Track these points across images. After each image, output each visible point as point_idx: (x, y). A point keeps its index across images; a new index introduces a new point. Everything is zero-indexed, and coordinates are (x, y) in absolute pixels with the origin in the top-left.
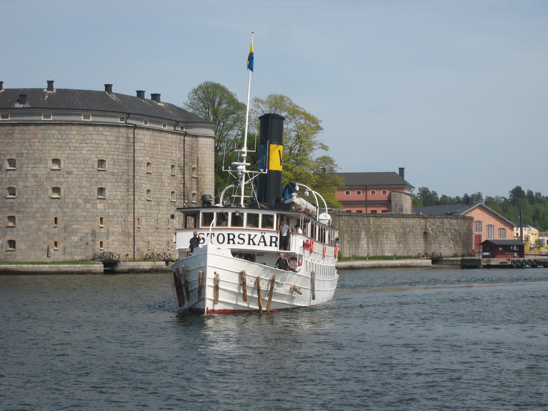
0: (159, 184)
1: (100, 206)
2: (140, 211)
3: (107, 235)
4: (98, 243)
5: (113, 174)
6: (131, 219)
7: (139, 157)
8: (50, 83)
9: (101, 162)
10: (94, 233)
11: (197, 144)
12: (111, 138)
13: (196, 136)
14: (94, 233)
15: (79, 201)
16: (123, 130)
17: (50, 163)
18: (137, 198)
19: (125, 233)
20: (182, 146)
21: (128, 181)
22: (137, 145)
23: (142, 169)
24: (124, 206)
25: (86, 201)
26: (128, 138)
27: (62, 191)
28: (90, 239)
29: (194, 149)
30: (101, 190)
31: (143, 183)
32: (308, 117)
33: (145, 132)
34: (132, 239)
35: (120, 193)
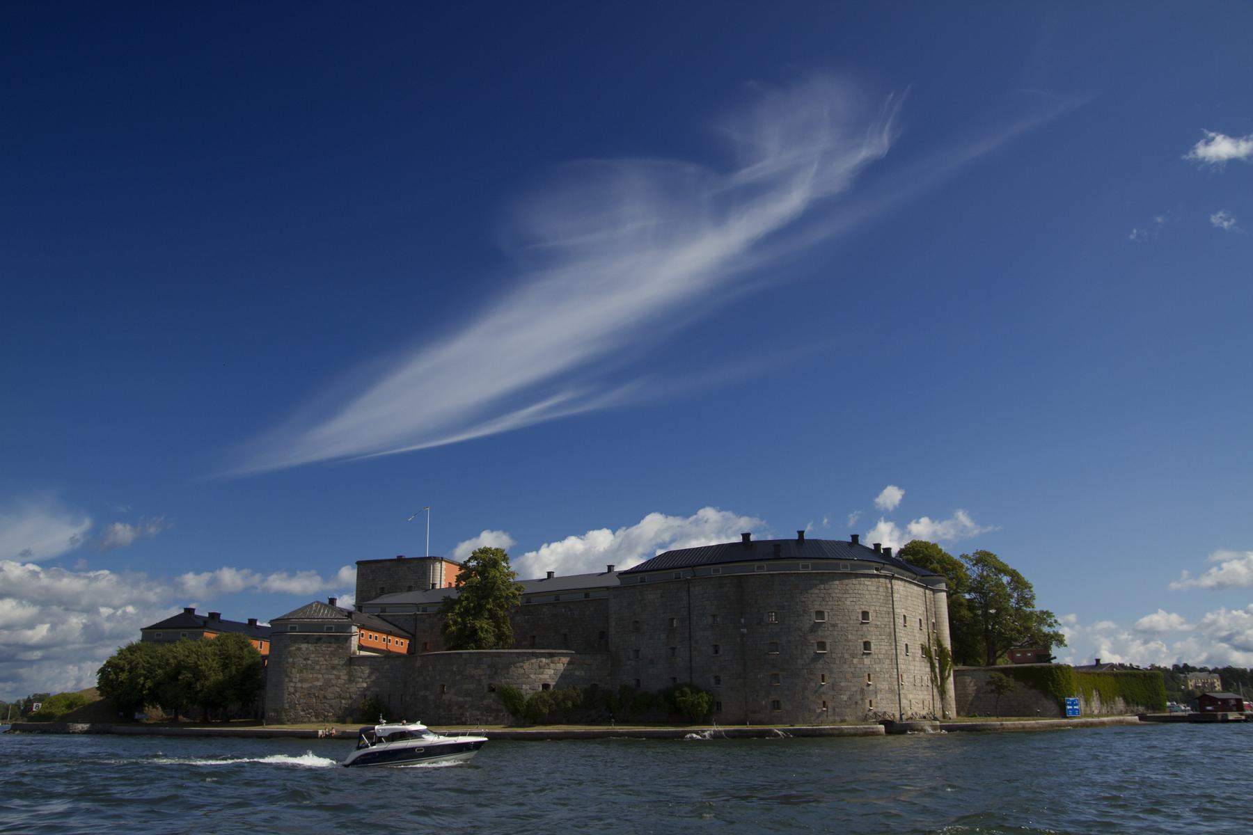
2: (901, 666)
4: (867, 701)
5: (877, 626)
7: (900, 611)
8: (801, 533)
12: (873, 588)
14: (862, 691)
15: (846, 656)
16: (882, 580)
17: (814, 615)
19: (891, 691)
23: (900, 621)
24: (888, 661)
27: (828, 647)
28: (859, 697)
29: (935, 602)
30: (867, 645)
31: (903, 639)
32: (1014, 575)
35: (884, 647)
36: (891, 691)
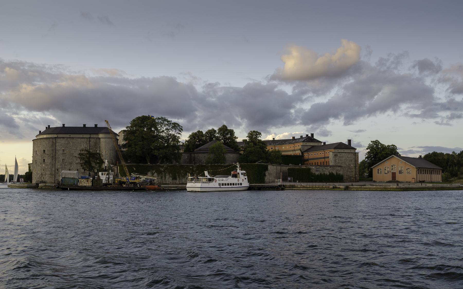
0: (71, 157)
1: (44, 165)
3: (45, 175)
6: (54, 169)
7: (58, 148)
9: (44, 151)
10: (42, 174)
11: (100, 142)
13: (99, 139)
18: (57, 162)
19: (51, 174)
20: (88, 142)
21: (53, 156)
22: (57, 144)
25: (41, 164)
26: (53, 142)
30: (44, 160)
33: (62, 139)
34: (54, 176)
36: (51, 174)
